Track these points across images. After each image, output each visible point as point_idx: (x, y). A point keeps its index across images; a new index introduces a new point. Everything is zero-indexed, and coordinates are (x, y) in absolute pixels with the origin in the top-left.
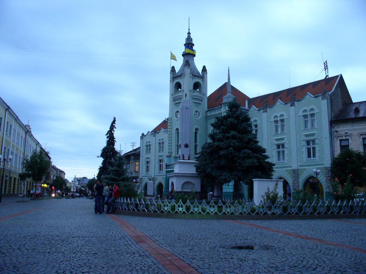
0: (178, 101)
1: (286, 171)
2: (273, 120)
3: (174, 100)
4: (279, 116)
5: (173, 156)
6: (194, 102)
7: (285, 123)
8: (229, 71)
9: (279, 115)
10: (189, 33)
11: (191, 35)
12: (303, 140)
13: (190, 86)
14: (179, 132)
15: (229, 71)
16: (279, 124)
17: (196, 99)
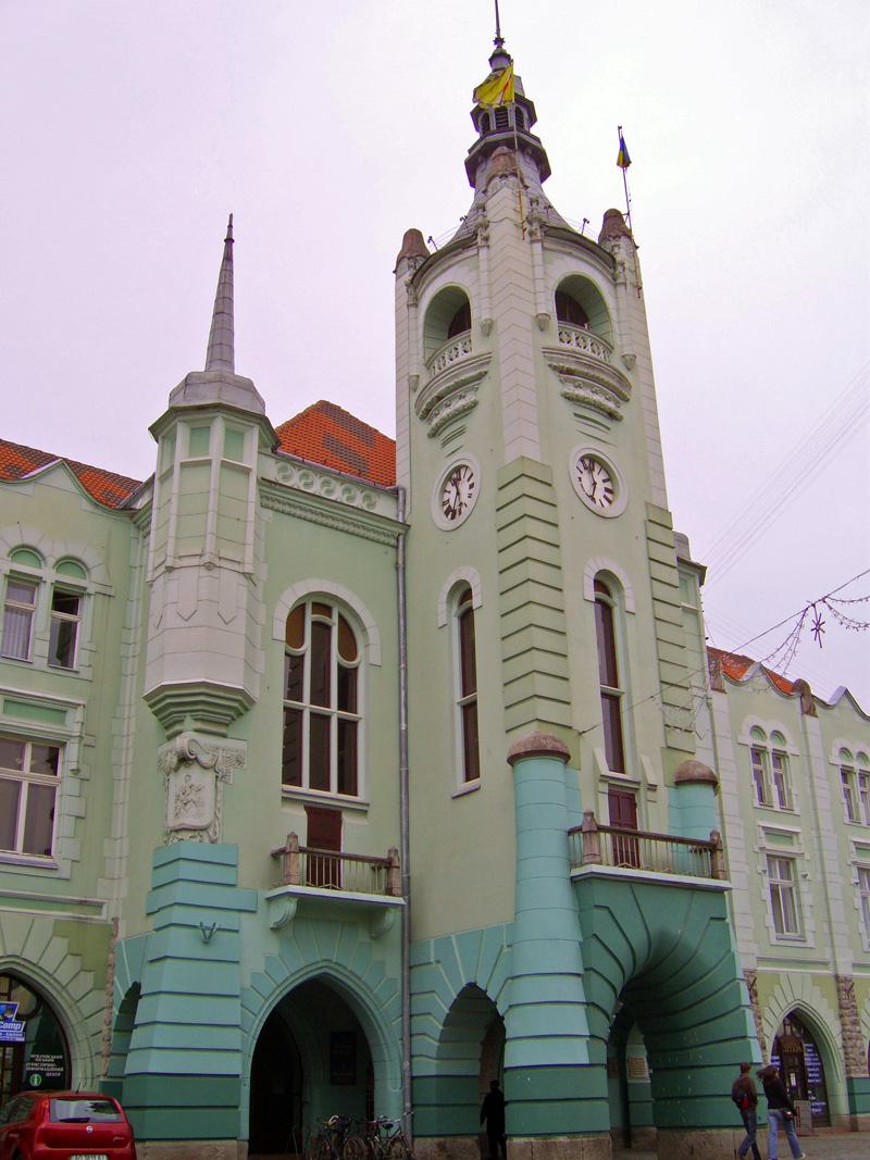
0: (611, 405)
1: (816, 979)
2: (751, 740)
3: (569, 372)
7: (793, 767)
9: (768, 729)
10: (500, 58)
12: (855, 863)
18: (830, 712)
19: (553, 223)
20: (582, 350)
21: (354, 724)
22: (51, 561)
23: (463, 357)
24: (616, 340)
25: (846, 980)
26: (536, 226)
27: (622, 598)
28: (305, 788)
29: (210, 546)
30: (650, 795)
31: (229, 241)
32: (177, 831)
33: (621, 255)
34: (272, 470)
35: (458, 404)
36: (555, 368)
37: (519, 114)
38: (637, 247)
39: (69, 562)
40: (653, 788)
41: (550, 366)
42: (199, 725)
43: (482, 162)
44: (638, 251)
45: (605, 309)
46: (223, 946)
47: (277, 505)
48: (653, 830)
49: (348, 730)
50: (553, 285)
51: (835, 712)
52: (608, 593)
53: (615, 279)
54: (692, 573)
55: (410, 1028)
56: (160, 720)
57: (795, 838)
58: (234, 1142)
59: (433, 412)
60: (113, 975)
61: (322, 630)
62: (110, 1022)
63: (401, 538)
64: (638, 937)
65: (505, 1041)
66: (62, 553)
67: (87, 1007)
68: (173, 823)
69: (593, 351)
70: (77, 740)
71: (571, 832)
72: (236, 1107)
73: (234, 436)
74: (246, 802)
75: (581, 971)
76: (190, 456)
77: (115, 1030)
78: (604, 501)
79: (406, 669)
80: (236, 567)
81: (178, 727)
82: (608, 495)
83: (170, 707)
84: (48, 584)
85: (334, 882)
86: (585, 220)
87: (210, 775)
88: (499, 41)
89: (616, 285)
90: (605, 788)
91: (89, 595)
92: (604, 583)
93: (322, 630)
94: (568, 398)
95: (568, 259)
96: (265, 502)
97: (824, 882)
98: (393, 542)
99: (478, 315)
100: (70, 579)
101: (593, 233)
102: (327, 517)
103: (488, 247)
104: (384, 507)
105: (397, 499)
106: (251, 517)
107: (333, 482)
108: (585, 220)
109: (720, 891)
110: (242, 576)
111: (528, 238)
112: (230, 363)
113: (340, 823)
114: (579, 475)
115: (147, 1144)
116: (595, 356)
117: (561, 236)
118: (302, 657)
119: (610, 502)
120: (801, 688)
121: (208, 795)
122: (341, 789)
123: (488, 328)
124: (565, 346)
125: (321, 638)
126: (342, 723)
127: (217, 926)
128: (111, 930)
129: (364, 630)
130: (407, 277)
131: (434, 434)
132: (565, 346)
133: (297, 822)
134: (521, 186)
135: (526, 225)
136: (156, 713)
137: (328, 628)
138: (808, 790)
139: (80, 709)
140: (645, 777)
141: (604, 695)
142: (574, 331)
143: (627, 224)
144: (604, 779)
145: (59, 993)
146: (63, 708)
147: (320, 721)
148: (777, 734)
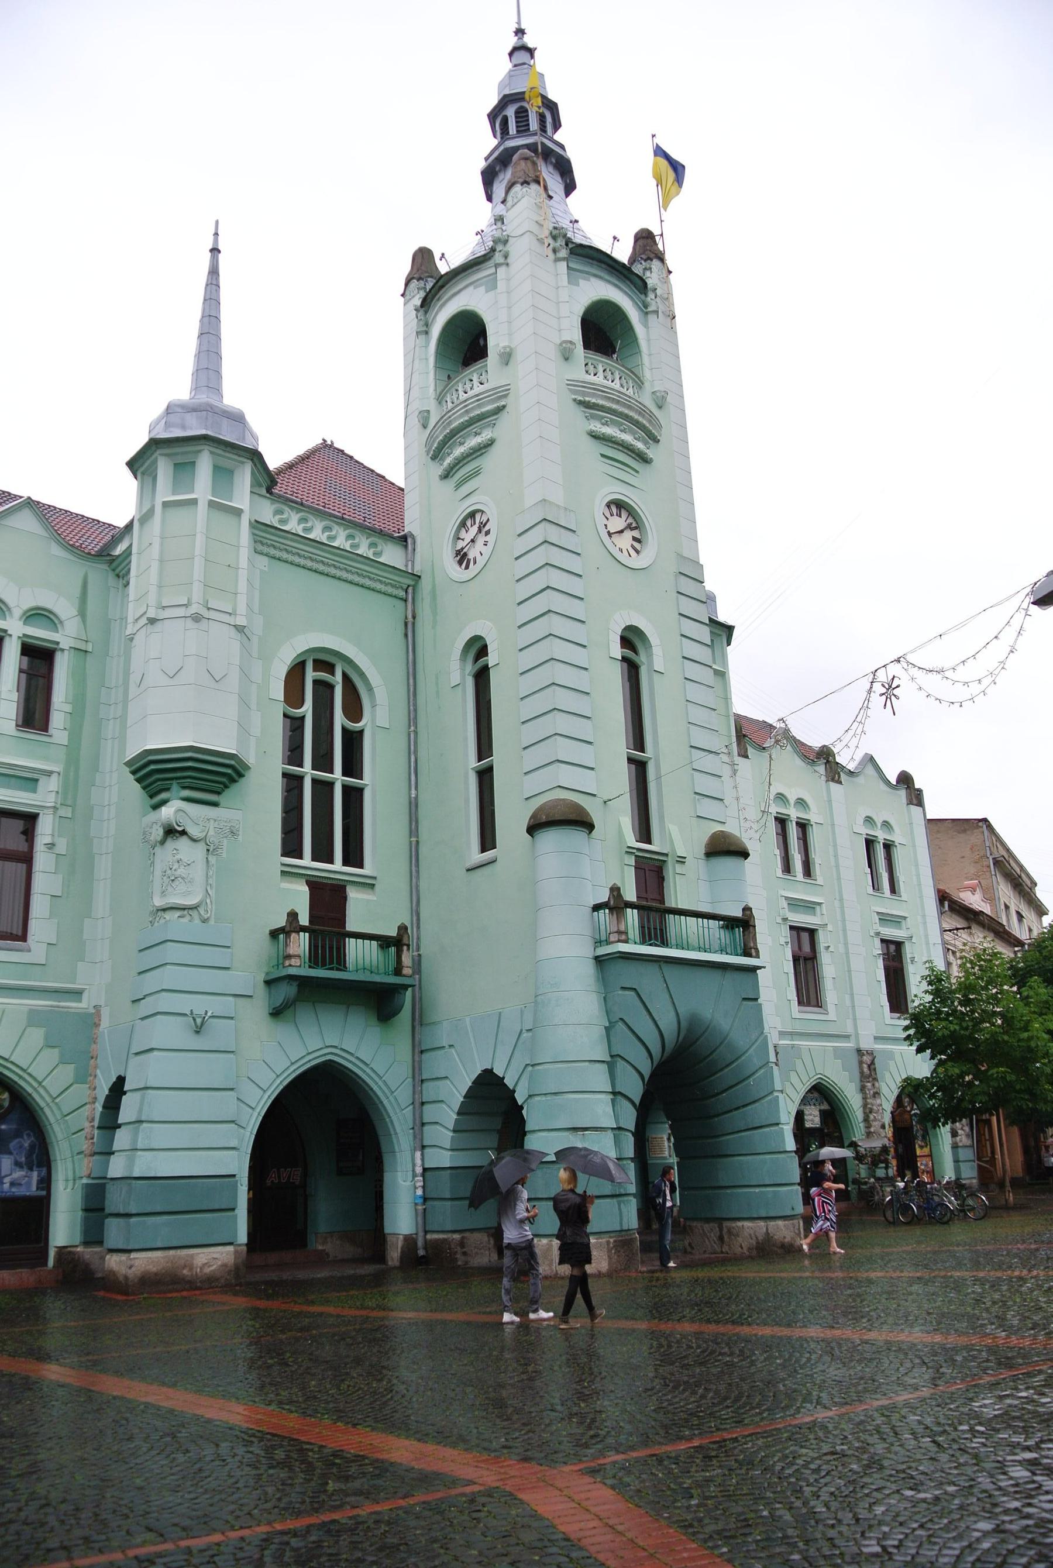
0: (640, 445)
1: (838, 1053)
4: (792, 802)
10: (522, 51)
16: (793, 832)
18: (855, 779)
19: (578, 240)
20: (609, 383)
21: (359, 791)
22: (17, 613)
23: (478, 389)
24: (647, 375)
25: (870, 1053)
26: (561, 242)
27: (650, 655)
28: (307, 861)
29: (197, 595)
30: (679, 868)
32: (164, 910)
33: (652, 279)
34: (267, 512)
35: (473, 442)
36: (581, 403)
37: (542, 118)
38: (670, 272)
39: (38, 615)
40: (681, 860)
41: (575, 400)
42: (187, 793)
43: (500, 171)
44: (671, 276)
45: (634, 339)
46: (220, 1034)
47: (272, 551)
48: (682, 905)
49: (354, 797)
50: (580, 310)
51: (860, 780)
52: (634, 649)
53: (646, 307)
54: (719, 632)
55: (421, 1117)
56: (144, 788)
57: (818, 908)
58: (231, 1248)
59: (446, 450)
60: (96, 1067)
61: (324, 689)
62: (93, 1120)
63: (410, 590)
64: (668, 1022)
65: (525, 1134)
66: (28, 603)
67: (68, 1102)
68: (158, 902)
69: (622, 385)
70: (51, 811)
71: (596, 908)
72: (233, 1209)
73: (222, 475)
74: (243, 877)
75: (608, 1059)
76: (173, 494)
77: (99, 1128)
79: (416, 732)
81: (163, 796)
82: (636, 544)
83: (158, 774)
84: (15, 638)
85: (339, 963)
86: (615, 238)
87: (201, 847)
88: (520, 32)
89: (647, 313)
90: (632, 861)
91: (63, 650)
92: (631, 639)
93: (324, 689)
94: (595, 436)
96: (260, 547)
97: (847, 953)
98: (402, 594)
99: (495, 342)
100: (39, 633)
101: (623, 253)
102: (329, 565)
103: (507, 264)
104: (392, 555)
105: (406, 547)
106: (244, 562)
107: (336, 528)
108: (615, 238)
109: (754, 969)
110: (233, 629)
111: (551, 256)
112: (218, 390)
113: (345, 898)
114: (606, 522)
115: (133, 1255)
116: (624, 390)
117: (590, 257)
118: (302, 718)
119: (637, 552)
120: (825, 755)
121: (198, 872)
122: (346, 862)
123: (507, 357)
124: (591, 378)
125: (322, 697)
126: (347, 789)
127: (209, 1014)
128: (91, 1020)
129: (370, 689)
130: (417, 301)
131: (446, 476)
132: (591, 378)
133: (299, 899)
134: (545, 196)
135: (550, 240)
136: (138, 780)
137: (331, 687)
138: (832, 859)
139: (54, 777)
140: (674, 850)
141: (631, 760)
142: (601, 362)
143: (660, 247)
145: (35, 1089)
146: (35, 776)
147: (323, 789)
148: (801, 803)
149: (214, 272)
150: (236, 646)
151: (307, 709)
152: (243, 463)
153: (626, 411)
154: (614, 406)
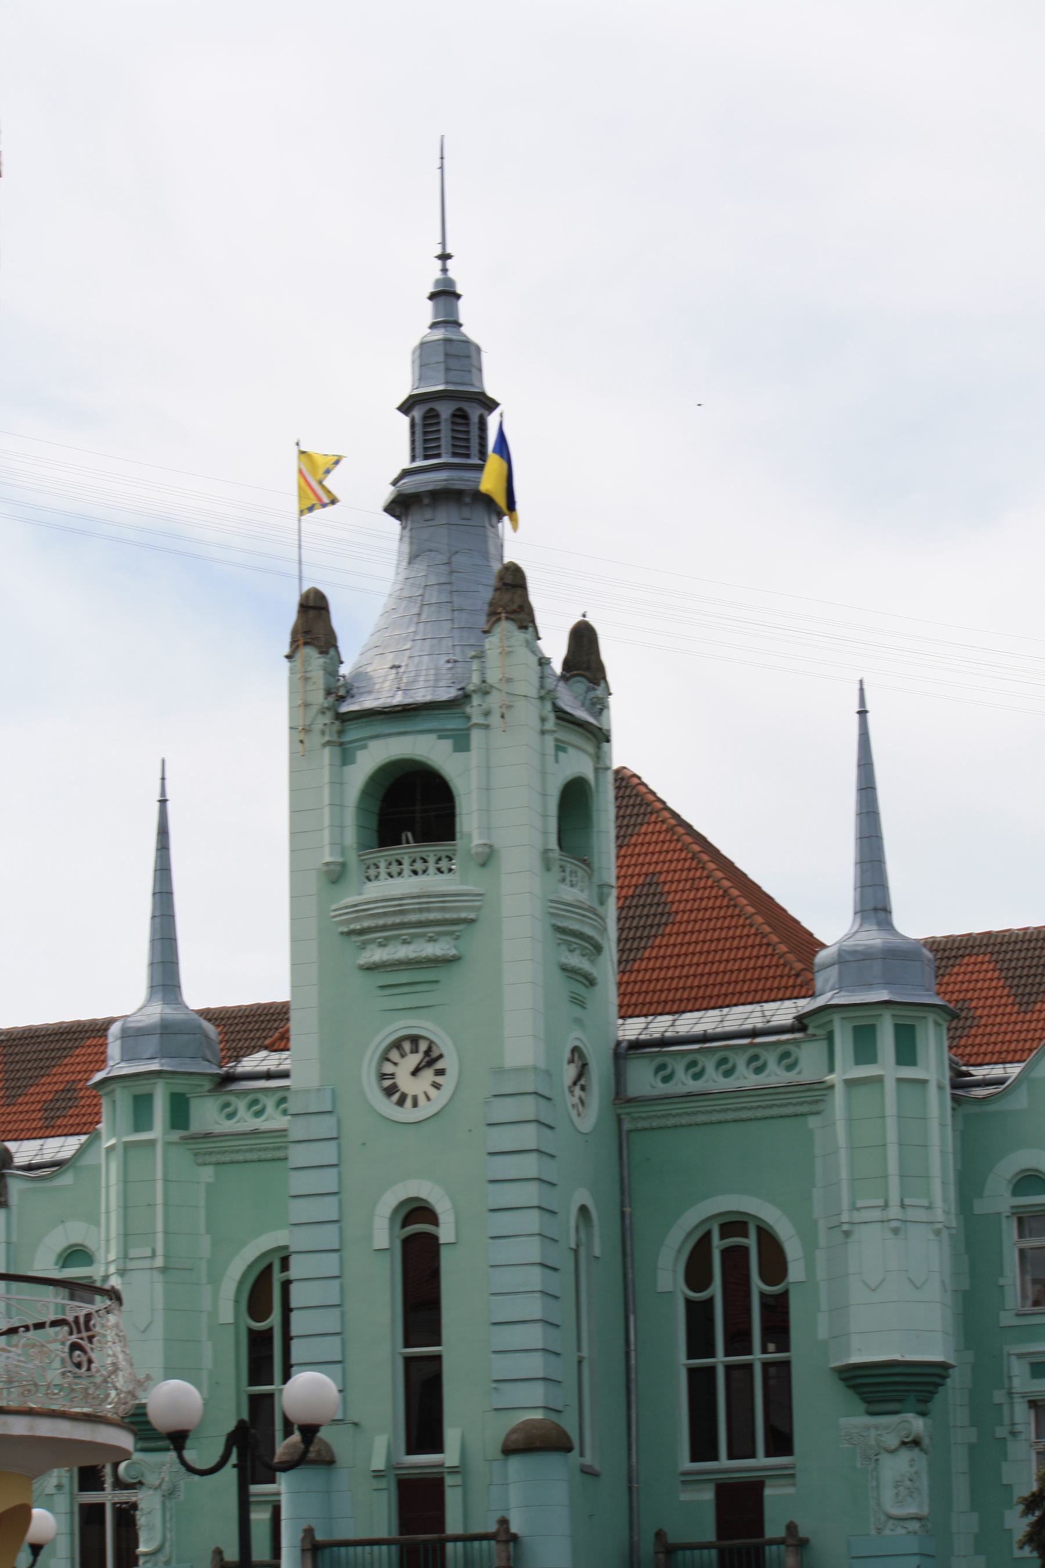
0: (430, 950)
3: (362, 932)
5: (379, 1463)
6: (565, 969)
8: (863, 713)
11: (465, 311)
13: (545, 816)
14: (445, 1233)
15: (863, 713)
17: (580, 936)
31: (163, 802)
34: (207, 1114)
40: (454, 1471)
41: (342, 933)
47: (213, 1159)
78: (433, 1092)
80: (147, 1264)
88: (444, 257)
89: (469, 729)
95: (373, 745)
110: (155, 1272)
144: (378, 1475)
149: (163, 832)
150: (159, 1289)
151: (275, 1319)
152: (155, 1084)
153: (398, 920)
154: (381, 922)
